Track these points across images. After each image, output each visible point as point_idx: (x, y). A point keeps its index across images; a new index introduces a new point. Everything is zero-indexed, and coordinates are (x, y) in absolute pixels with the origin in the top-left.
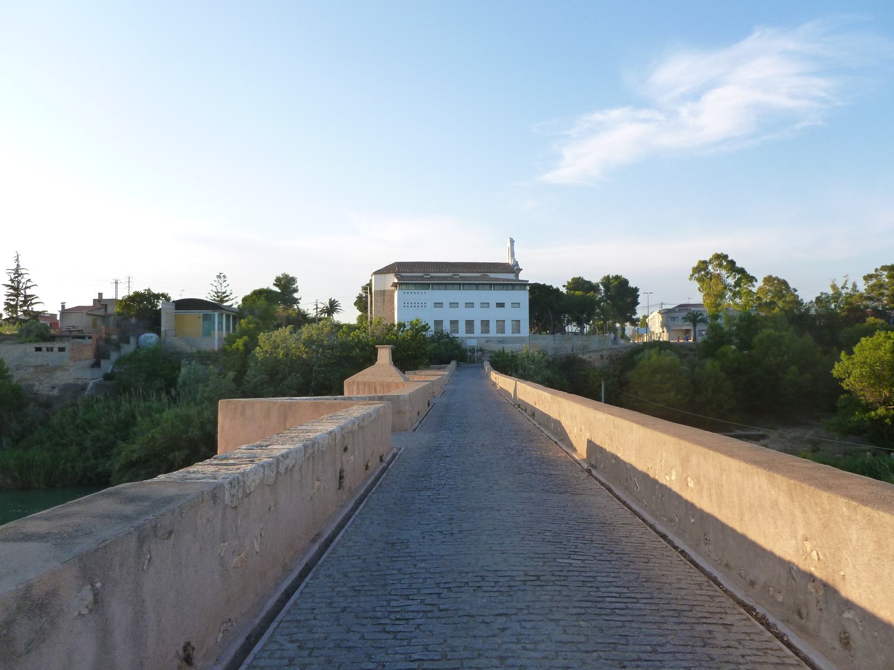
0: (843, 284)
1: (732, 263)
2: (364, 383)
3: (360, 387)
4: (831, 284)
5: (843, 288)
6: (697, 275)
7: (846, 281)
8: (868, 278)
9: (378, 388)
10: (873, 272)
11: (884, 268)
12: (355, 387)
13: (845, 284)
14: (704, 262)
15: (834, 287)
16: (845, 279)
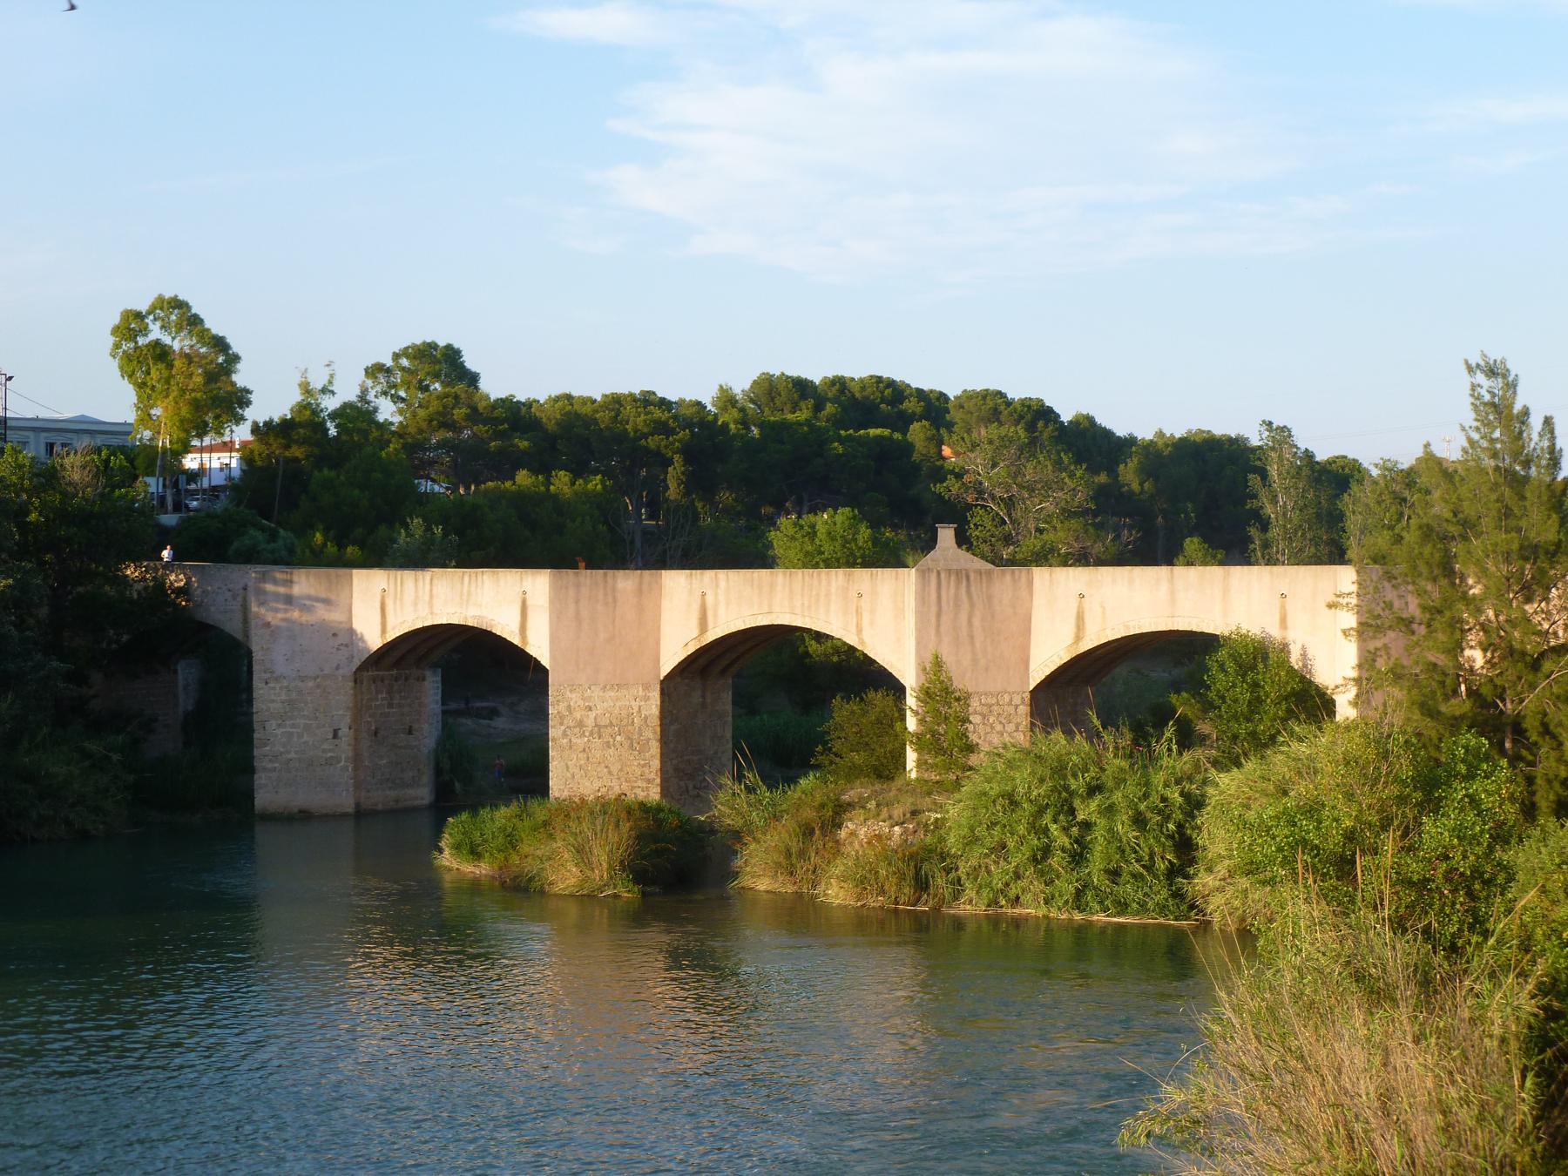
0: (326, 382)
1: (194, 322)
2: (949, 571)
3: (943, 575)
4: (298, 379)
5: (324, 391)
6: (128, 346)
7: (332, 376)
8: (375, 371)
9: (972, 576)
10: (389, 363)
11: (405, 353)
12: (933, 577)
13: (330, 382)
14: (139, 316)
15: (306, 389)
16: (327, 371)
